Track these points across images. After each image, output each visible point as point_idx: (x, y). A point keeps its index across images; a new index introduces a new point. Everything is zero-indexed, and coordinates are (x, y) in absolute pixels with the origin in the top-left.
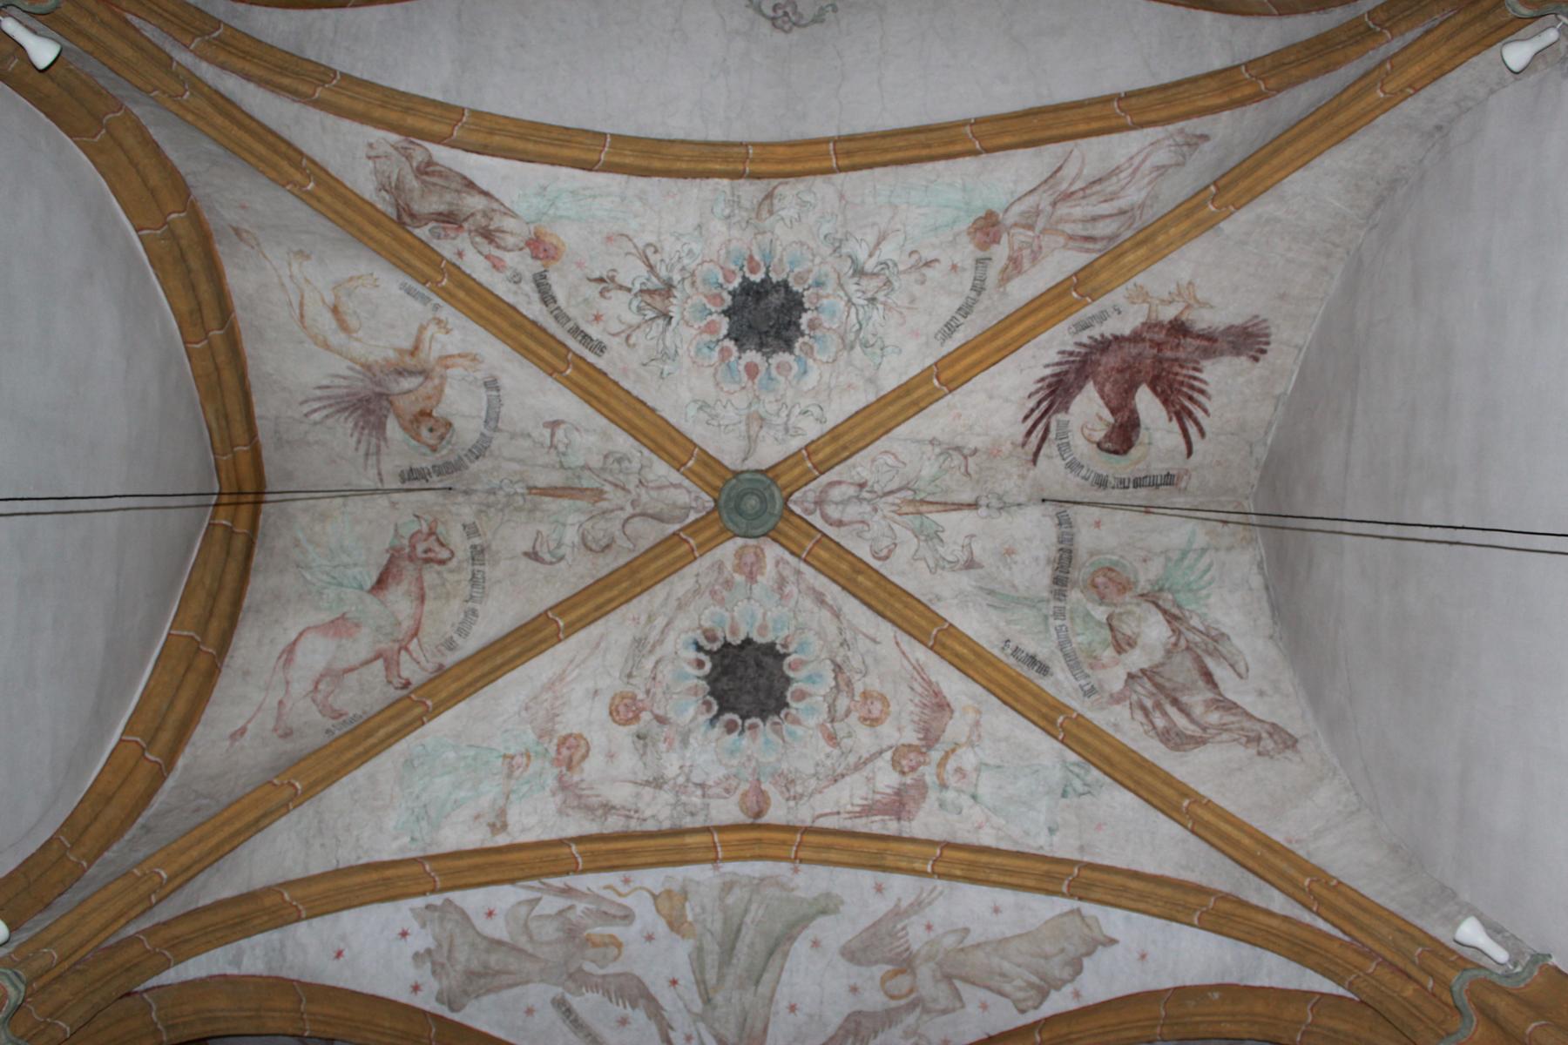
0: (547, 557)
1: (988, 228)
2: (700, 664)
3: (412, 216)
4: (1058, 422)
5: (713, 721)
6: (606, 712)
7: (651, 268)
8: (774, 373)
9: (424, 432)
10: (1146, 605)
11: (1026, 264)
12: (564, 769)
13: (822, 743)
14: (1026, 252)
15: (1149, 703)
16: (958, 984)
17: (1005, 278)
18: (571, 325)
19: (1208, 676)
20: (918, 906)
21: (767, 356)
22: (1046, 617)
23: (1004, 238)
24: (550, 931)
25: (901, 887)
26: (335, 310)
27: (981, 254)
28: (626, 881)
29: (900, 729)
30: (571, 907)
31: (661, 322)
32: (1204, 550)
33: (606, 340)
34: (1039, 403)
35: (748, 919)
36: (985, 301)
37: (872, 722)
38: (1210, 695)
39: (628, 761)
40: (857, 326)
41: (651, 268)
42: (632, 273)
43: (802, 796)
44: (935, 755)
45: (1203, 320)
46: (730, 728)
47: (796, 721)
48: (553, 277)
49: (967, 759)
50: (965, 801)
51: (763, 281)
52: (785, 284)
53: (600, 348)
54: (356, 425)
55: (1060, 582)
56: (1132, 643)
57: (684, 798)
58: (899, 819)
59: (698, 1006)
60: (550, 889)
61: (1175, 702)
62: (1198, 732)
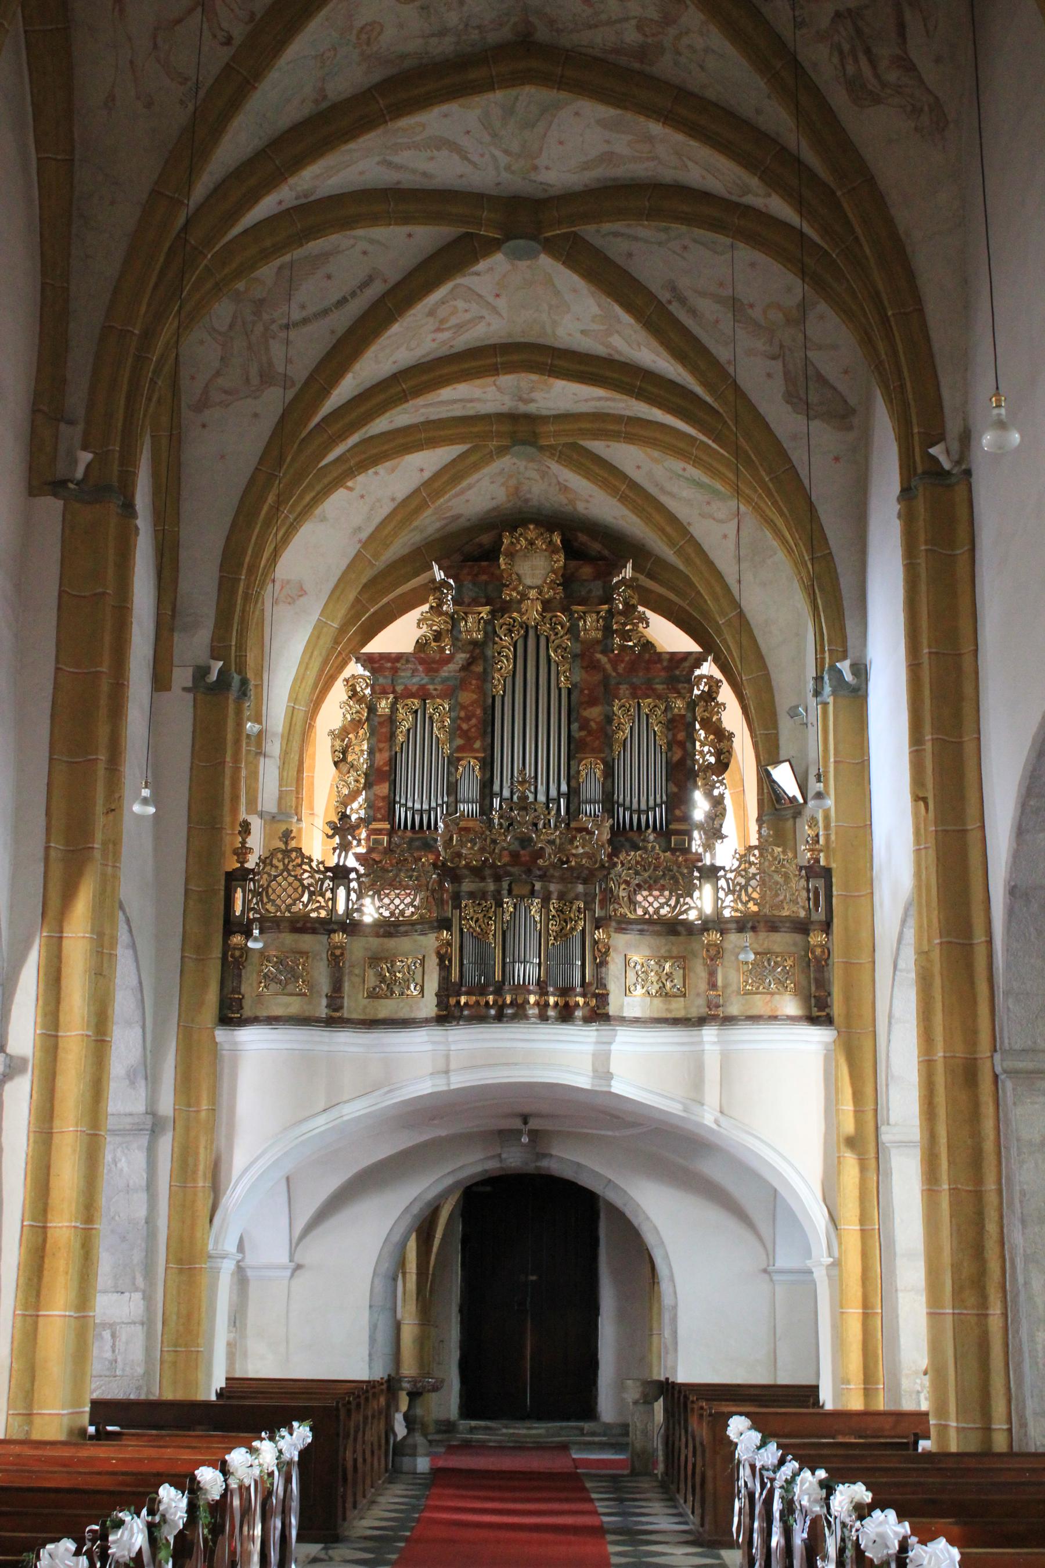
15: (846, 47)
19: (901, 28)
61: (868, 51)
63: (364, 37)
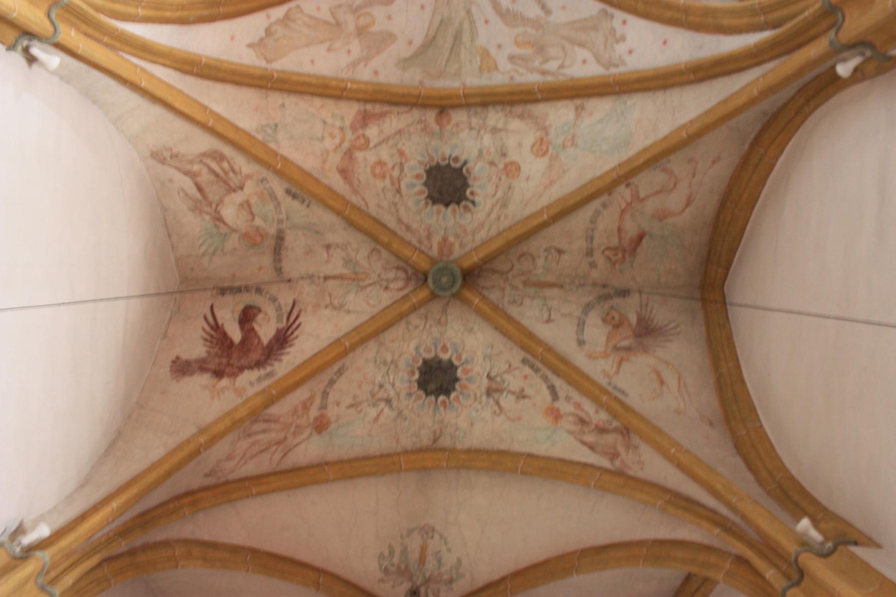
0: (553, 251)
1: (321, 426)
2: (472, 193)
3: (622, 433)
4: (282, 323)
5: (465, 163)
6: (523, 168)
7: (497, 403)
8: (433, 348)
9: (617, 317)
10: (234, 226)
11: (300, 407)
12: (545, 139)
13: (407, 152)
14: (300, 412)
15: (231, 174)
16: (333, 21)
17: (311, 399)
18: (540, 374)
19: (200, 189)
20: (355, 64)
21: (436, 356)
22: (288, 218)
23: (312, 420)
24: (553, 52)
25: (365, 74)
26: (662, 382)
27: (324, 411)
28: (512, 78)
29: (365, 159)
30: (542, 63)
31: (493, 374)
32: (204, 255)
33: (521, 365)
34: (292, 333)
35: (446, 56)
36: (322, 387)
37: (380, 163)
38: (199, 179)
39: (511, 142)
40: (389, 372)
41: (497, 403)
42: (507, 401)
43: (418, 123)
44: (346, 145)
45: (205, 379)
46: (456, 159)
47: (421, 163)
48: (549, 398)
49: (329, 144)
50: (330, 121)
51: (439, 395)
52: (427, 394)
53: (524, 361)
54: (652, 321)
55: (280, 238)
56: (241, 205)
57: (481, 122)
58: (365, 111)
59: (474, 9)
60: (553, 74)
61: (217, 175)
62: (205, 160)
63: (544, 147)
